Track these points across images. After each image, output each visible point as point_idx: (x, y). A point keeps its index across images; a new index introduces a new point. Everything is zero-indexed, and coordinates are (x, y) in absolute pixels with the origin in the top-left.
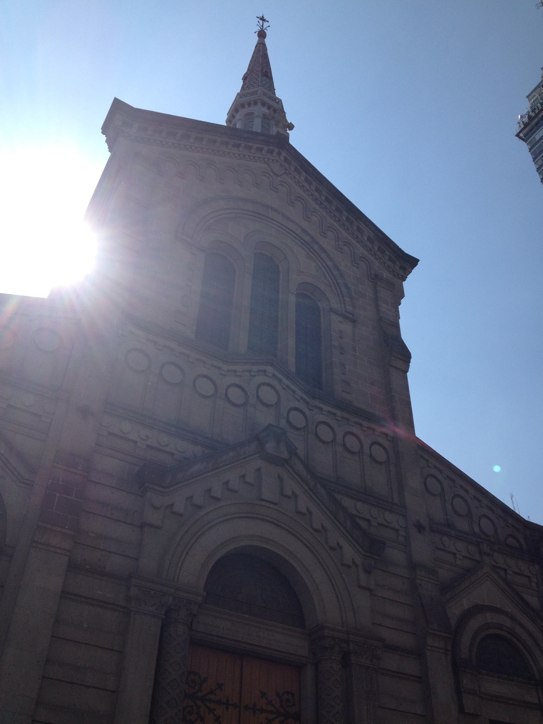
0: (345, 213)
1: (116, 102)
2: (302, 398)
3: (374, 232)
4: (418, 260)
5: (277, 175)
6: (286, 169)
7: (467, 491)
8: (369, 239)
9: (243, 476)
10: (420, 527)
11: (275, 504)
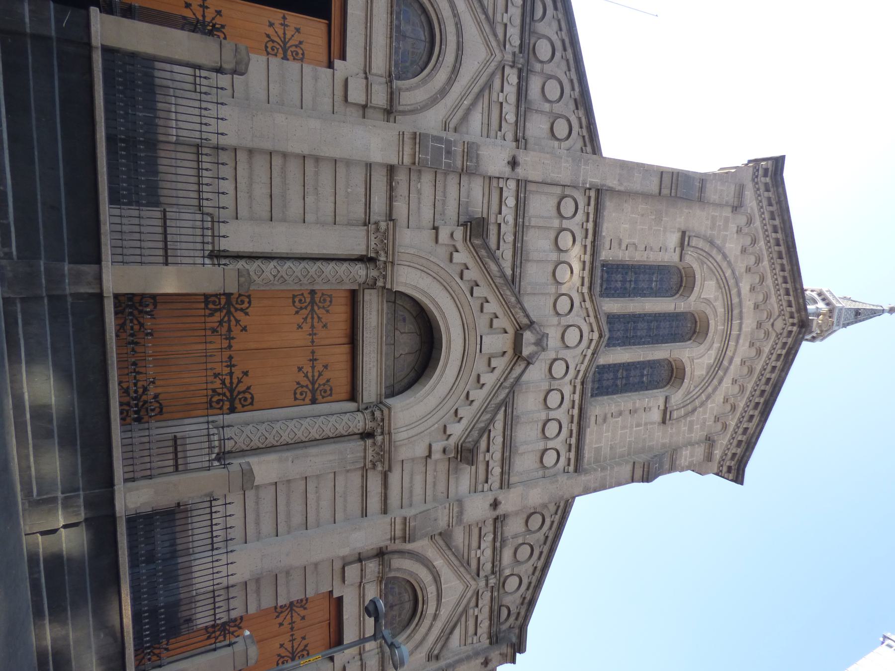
0: (762, 400)
2: (579, 371)
3: (754, 433)
4: (742, 483)
5: (773, 325)
6: (781, 334)
7: (539, 558)
8: (746, 429)
10: (495, 504)
11: (481, 351)
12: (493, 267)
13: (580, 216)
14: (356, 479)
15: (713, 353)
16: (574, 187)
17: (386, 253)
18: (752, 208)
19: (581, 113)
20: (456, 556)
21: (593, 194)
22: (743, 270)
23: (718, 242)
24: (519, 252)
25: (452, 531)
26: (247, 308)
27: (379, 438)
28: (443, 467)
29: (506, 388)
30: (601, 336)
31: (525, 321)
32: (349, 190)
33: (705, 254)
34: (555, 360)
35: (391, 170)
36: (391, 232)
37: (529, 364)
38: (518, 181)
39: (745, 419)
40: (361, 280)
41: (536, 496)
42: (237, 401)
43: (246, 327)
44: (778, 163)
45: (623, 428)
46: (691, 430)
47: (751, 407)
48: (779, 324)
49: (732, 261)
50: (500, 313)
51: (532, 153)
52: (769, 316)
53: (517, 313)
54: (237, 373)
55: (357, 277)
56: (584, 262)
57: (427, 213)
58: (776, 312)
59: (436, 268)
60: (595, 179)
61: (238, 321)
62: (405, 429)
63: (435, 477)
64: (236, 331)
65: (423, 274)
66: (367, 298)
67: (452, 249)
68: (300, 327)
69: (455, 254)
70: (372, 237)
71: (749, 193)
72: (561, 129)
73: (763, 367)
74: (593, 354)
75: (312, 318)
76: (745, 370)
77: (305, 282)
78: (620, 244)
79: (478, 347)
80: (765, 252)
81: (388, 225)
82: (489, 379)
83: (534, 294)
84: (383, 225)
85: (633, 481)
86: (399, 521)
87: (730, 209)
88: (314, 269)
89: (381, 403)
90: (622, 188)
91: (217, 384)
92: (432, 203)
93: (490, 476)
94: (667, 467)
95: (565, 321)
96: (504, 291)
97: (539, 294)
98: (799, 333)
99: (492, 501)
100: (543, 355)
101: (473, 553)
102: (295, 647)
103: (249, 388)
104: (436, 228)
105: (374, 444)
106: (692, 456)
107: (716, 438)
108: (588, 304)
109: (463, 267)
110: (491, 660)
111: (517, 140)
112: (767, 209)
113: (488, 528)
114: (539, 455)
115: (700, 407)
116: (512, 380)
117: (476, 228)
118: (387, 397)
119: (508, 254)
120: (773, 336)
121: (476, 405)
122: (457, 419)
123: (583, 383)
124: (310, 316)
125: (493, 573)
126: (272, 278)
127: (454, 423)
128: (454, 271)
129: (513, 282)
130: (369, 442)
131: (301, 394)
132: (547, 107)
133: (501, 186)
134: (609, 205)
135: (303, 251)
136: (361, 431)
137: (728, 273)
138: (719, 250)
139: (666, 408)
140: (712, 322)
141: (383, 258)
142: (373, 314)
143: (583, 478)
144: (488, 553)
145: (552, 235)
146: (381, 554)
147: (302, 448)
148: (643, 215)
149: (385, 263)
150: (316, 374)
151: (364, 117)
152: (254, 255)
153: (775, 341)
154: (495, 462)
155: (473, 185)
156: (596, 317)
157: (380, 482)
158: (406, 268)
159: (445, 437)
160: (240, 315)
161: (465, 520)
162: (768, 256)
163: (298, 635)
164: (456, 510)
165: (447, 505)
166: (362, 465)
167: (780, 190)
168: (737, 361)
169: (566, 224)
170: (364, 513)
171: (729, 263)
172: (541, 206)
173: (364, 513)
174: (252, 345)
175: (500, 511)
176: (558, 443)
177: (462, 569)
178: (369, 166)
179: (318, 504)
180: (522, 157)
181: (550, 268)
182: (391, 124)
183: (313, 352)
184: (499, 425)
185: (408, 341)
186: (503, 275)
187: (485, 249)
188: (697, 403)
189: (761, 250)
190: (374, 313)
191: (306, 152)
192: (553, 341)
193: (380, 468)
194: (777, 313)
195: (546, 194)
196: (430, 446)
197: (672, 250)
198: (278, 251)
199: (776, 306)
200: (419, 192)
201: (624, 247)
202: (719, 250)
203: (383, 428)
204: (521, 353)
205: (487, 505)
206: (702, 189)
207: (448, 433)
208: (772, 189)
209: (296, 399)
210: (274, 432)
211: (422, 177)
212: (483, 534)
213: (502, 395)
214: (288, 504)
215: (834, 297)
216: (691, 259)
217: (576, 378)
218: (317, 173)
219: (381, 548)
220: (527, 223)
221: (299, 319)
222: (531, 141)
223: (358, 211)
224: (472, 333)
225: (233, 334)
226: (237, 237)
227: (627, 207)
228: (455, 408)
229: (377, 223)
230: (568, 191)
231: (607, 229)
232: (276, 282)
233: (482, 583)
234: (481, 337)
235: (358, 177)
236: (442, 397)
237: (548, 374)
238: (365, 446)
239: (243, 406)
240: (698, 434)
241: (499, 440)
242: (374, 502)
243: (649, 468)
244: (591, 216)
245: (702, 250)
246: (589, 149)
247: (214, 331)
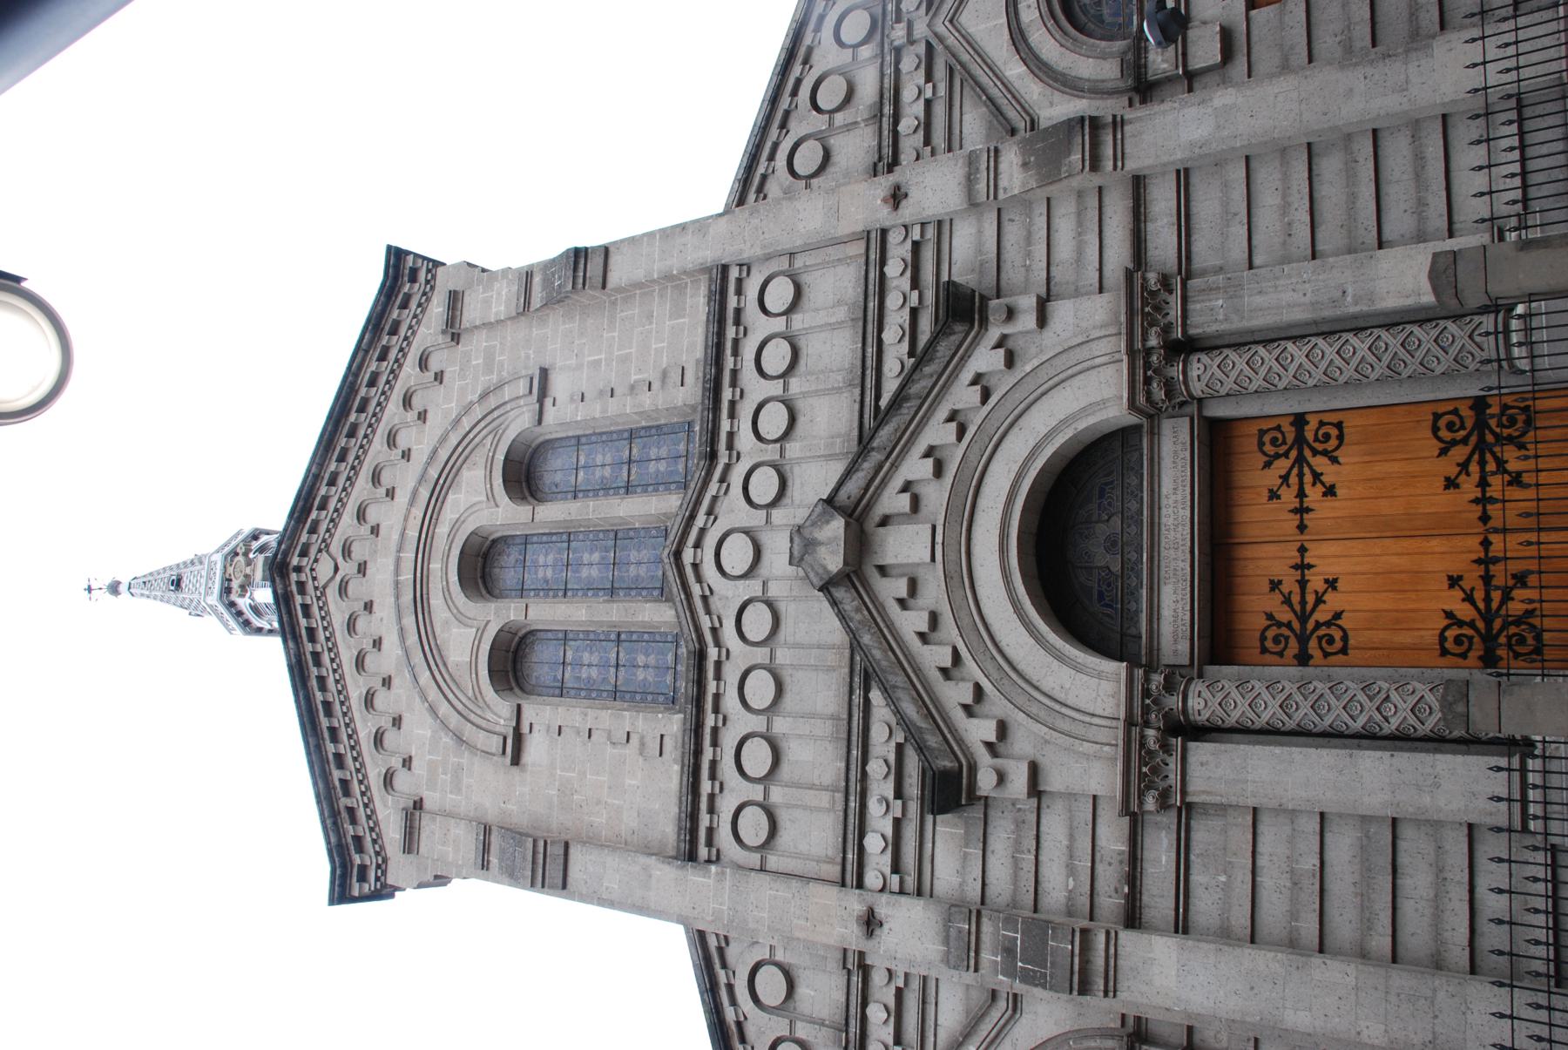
1: (332, 902)
2: (722, 480)
4: (389, 248)
5: (336, 569)
6: (320, 551)
9: (902, 602)
10: (897, 197)
12: (910, 710)
13: (727, 806)
14: (1203, 252)
15: (448, 515)
16: (740, 867)
17: (1142, 745)
18: (385, 806)
19: (730, 1015)
20: (977, 83)
21: (703, 852)
22: (395, 682)
23: (447, 740)
24: (854, 738)
25: (988, 137)
26: (1446, 628)
27: (1153, 342)
28: (1012, 275)
29: (879, 449)
30: (678, 554)
31: (840, 593)
32: (1223, 878)
33: (472, 717)
34: (774, 503)
35: (1133, 917)
36: (1134, 790)
37: (830, 501)
38: (860, 885)
39: (383, 379)
40: (1197, 686)
41: (804, 216)
42: (1469, 424)
43: (1451, 586)
44: (341, 893)
45: (625, 359)
46: (489, 357)
47: (373, 403)
48: (324, 569)
49: (418, 699)
50: (894, 610)
51: (832, 942)
52: (343, 590)
53: (858, 610)
54: (1469, 488)
55: (1206, 694)
56: (716, 710)
57: (1055, 826)
58: (332, 592)
59: (1034, 709)
60: (699, 880)
61: (1469, 598)
62: (1098, 361)
63: (1029, 254)
64: (1472, 579)
65: (1061, 696)
66: (1184, 646)
67: (1001, 748)
68: (1332, 584)
69: (992, 738)
70: (1174, 779)
71: (392, 833)
72: (771, 986)
73: (352, 484)
74: (692, 517)
75: (1303, 602)
76: (386, 478)
77: (1320, 685)
78: (642, 744)
79: (939, 539)
80: (357, 716)
81: (1141, 803)
82: (916, 467)
83: (819, 647)
84: (1150, 803)
85: (606, 251)
86: (1108, 165)
87: (427, 805)
88: (1301, 713)
89: (1150, 417)
90: (643, 859)
91: (1511, 456)
92: (1044, 844)
93: (909, 258)
94: (537, 279)
95: (752, 588)
96: (888, 660)
97: (811, 647)
98: (286, 554)
99: (904, 203)
100: (800, 515)
103: (1443, 452)
104: (1035, 789)
105: (1166, 330)
106: (487, 302)
107: (440, 339)
108: (705, 623)
109: (977, 709)
111: (865, 969)
112: (356, 801)
113: (910, 143)
114: (806, 303)
115: (472, 404)
116: (866, 465)
117: (949, 790)
118: (1136, 429)
119: (878, 733)
120: (336, 547)
121: (942, 412)
122: (984, 382)
123: (713, 456)
124: (1309, 607)
125: (898, 52)
126: (1394, 696)
127: (991, 373)
128: (997, 704)
129: (863, 676)
130: (1178, 333)
131: (1327, 437)
132: (802, 1031)
133: (896, 878)
134: (666, 826)
135: (1324, 752)
136: (1194, 358)
137: (425, 678)
138: (444, 725)
139: (541, 401)
140: (454, 577)
141: (1151, 733)
142: (1173, 610)
143: (709, 252)
144: (908, 94)
145: (785, 770)
146: (1143, 88)
147: (1325, 321)
148: (598, 803)
149: (1147, 724)
150: (1293, 479)
151: (1190, 1029)
152: (1431, 745)
153: (332, 536)
154: (897, 287)
155: (955, 880)
156: (689, 595)
157: (1150, 245)
158: (1099, 712)
159: (1010, 344)
160: (1465, 611)
161: (961, 161)
162: (349, 708)
164: (981, 186)
165: (1001, 196)
166: (1190, 283)
167: (333, 840)
168: (402, 497)
169: (756, 792)
170: (1184, 178)
171: (424, 698)
172: (812, 833)
173: (1184, 178)
174: (1435, 544)
175: (885, 183)
176: (760, 326)
177: (965, 57)
178: (1182, 925)
179: (1284, 197)
180: (853, 936)
181: (789, 701)
182: (1131, 1013)
183: (1302, 528)
184: (891, 367)
185: (1097, 551)
186: (885, 691)
187: (928, 748)
188: (478, 412)
189: (365, 721)
190: (1167, 612)
191: (1317, 960)
192: (778, 548)
193: (1152, 277)
194: (329, 591)
195: (798, 856)
196: (1042, 321)
197: (535, 728)
198: (1379, 754)
199: (332, 607)
200: (1071, 870)
201: (634, 739)
202: (444, 725)
203: (1147, 365)
204: (847, 525)
205: (914, 194)
206: (486, 848)
207: (1001, 352)
208: (350, 840)
209: (1339, 425)
210: (1386, 358)
211: (1063, 900)
212: (921, 132)
213: (886, 433)
214: (1352, 198)
215: (221, 618)
216: (500, 709)
217: (728, 467)
218: (1294, 915)
219: (1143, 101)
220: (840, 796)
221: (1333, 601)
222: (833, 964)
223: (1203, 834)
224: (952, 567)
225: (1481, 570)
226: (1465, 785)
227: (629, 821)
228: (988, 407)
229: (1164, 802)
230: (754, 859)
231: (671, 776)
232: (1385, 686)
233: (921, 30)
234: (933, 559)
235: (1204, 906)
236: (1015, 430)
237: (789, 475)
238: (1184, 325)
239: (1455, 412)
240: (475, 345)
241: (890, 336)
242: (1162, 201)
243: (575, 278)
244: (704, 805)
245: (478, 727)
246: (713, 943)
247: (1521, 579)
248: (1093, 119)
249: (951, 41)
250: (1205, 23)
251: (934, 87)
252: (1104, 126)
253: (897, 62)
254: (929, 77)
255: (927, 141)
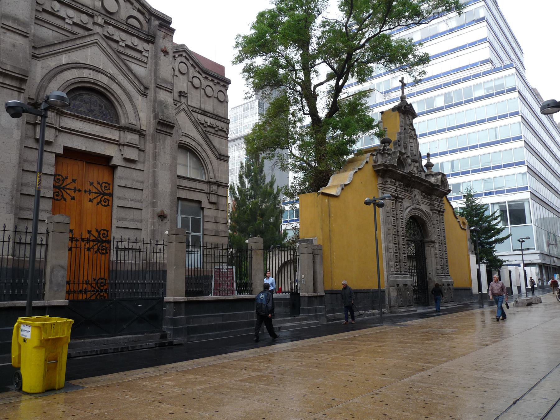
20: (64, 42)
101: (66, 26)
102: (96, 191)
110: (165, 48)
125: (92, 16)
144: (71, 13)
163: (88, 187)
177: (78, 42)
212: (50, 10)
233: (98, 29)
248: (22, 81)
249: (88, 39)
250: (56, 136)
251: (70, 24)
252: (21, 84)
253: (87, 14)
254: (75, 24)
255: (45, 11)
